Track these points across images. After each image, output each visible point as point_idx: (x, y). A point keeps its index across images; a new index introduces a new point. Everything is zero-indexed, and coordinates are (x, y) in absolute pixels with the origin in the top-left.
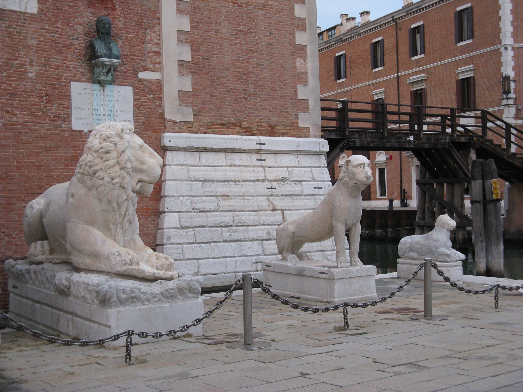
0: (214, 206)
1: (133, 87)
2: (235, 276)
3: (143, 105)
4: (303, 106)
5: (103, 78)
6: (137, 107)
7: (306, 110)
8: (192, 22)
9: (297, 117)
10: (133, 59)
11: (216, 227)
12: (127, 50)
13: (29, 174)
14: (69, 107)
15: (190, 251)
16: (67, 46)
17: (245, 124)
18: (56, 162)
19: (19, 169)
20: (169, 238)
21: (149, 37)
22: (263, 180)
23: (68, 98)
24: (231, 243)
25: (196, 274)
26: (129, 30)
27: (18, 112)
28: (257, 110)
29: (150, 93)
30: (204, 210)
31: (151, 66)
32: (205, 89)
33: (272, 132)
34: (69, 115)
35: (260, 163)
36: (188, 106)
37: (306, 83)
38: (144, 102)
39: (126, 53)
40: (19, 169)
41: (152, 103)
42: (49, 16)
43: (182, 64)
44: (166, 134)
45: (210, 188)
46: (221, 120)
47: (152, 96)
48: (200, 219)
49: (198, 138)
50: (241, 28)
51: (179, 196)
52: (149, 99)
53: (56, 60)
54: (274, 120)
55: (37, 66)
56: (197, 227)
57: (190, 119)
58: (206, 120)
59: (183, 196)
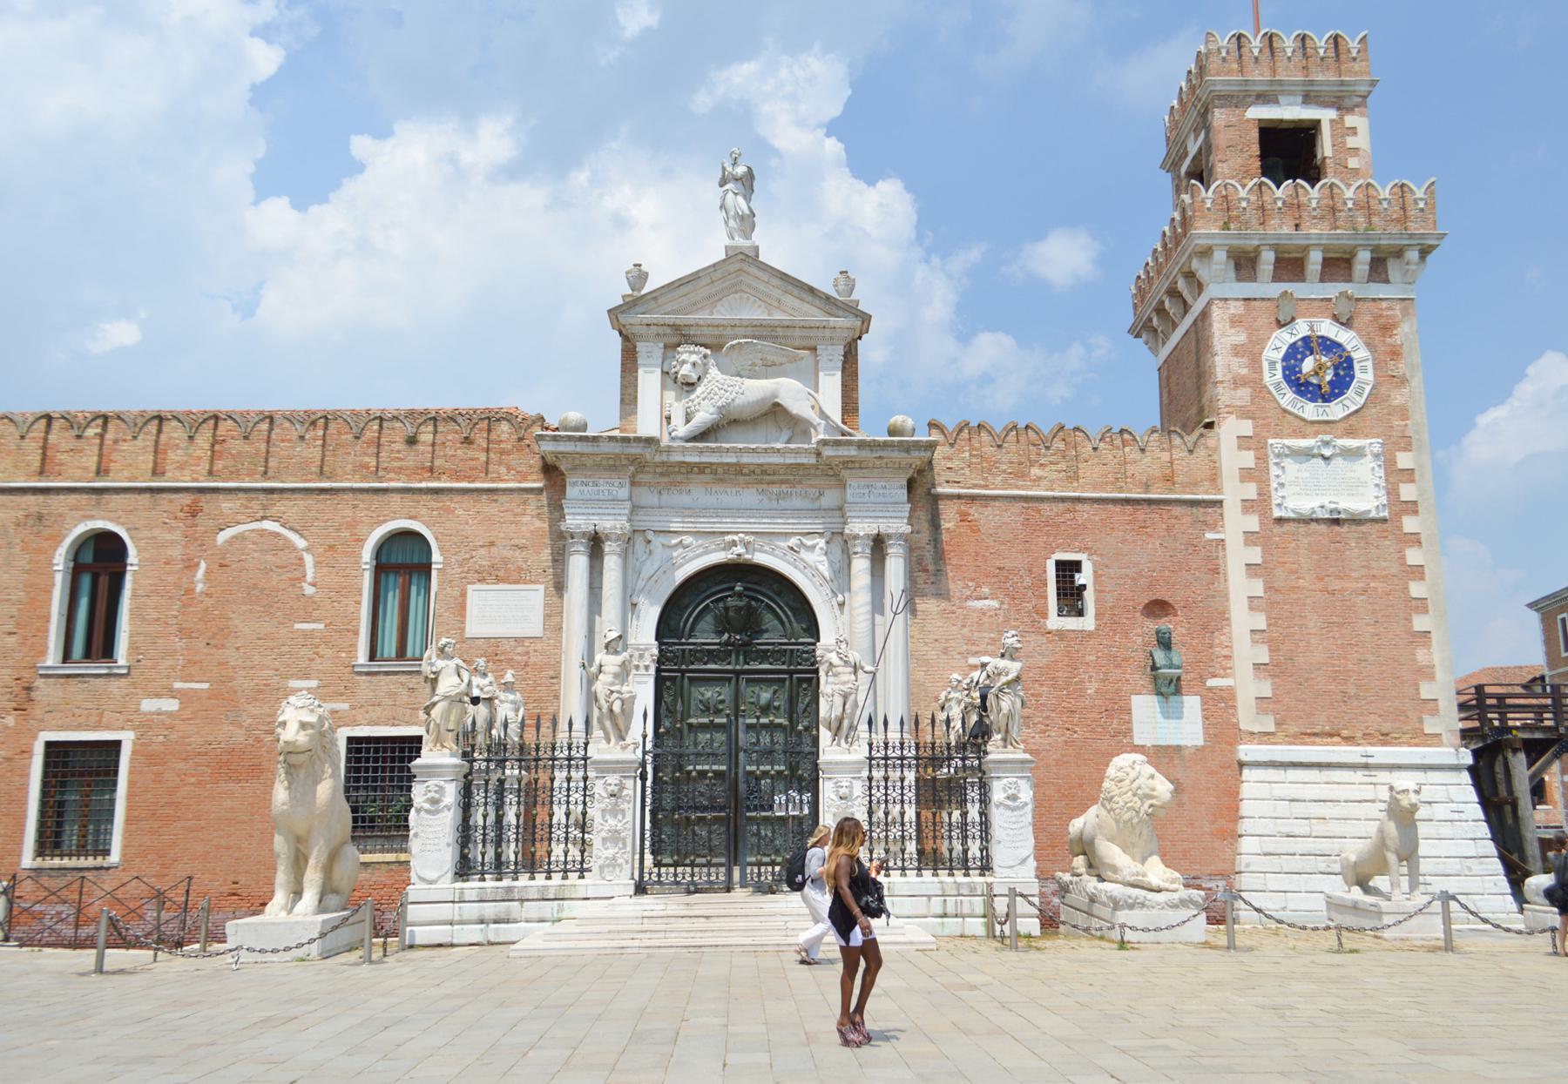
0: (1305, 830)
4: (1431, 706)
5: (1163, 690)
6: (1206, 718)
7: (1435, 712)
8: (1269, 618)
9: (1421, 721)
14: (1130, 722)
15: (1274, 882)
16: (1126, 660)
17: (1345, 733)
19: (1080, 786)
20: (1248, 865)
22: (1373, 801)
23: (1128, 711)
25: (1284, 909)
28: (1362, 715)
33: (1385, 739)
34: (1130, 730)
35: (1369, 780)
37: (1432, 677)
43: (1257, 666)
44: (1241, 747)
45: (1299, 809)
50: (1334, 619)
53: (1115, 674)
54: (1386, 727)
57: (1272, 728)
58: (1293, 729)
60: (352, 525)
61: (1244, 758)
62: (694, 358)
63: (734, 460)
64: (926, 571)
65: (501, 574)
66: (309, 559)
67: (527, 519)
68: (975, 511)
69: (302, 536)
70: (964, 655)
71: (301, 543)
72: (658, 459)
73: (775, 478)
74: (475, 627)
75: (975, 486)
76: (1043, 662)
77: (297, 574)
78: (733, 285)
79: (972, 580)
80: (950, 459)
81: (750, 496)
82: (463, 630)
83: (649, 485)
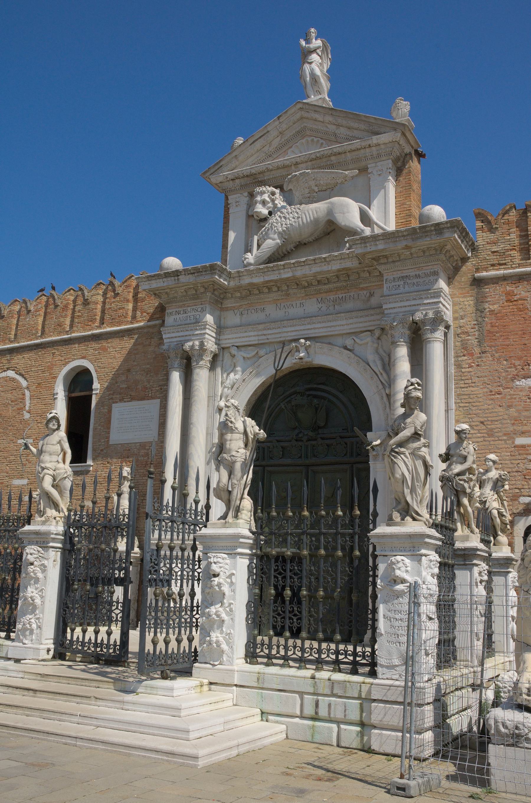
60: (50, 368)
62: (266, 197)
63: (289, 275)
64: (472, 355)
65: (133, 394)
66: (27, 393)
67: (151, 349)
68: (521, 290)
69: (25, 379)
70: (511, 435)
71: (24, 383)
72: (232, 284)
73: (331, 286)
74: (116, 436)
75: (520, 266)
77: (21, 405)
78: (298, 132)
79: (520, 358)
80: (495, 243)
81: (312, 306)
82: (108, 438)
83: (233, 309)
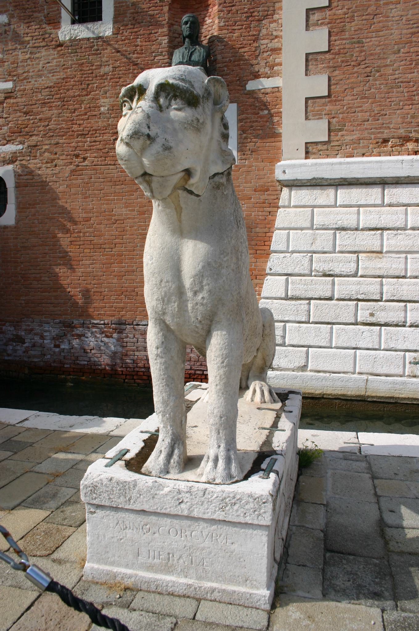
0: (351, 268)
1: (238, 104)
2: (367, 380)
3: (252, 127)
10: (239, 65)
11: (350, 300)
12: (230, 55)
13: (97, 226)
18: (129, 210)
21: (264, 31)
24: (372, 328)
26: (233, 28)
27: (88, 155)
29: (264, 108)
30: (331, 273)
31: (267, 69)
32: (353, 88)
36: (321, 118)
38: (254, 122)
39: (228, 59)
40: (88, 219)
41: (267, 122)
42: (126, 34)
46: (379, 133)
47: (266, 112)
48: (322, 287)
49: (340, 163)
51: (293, 252)
52: (261, 117)
55: (111, 97)
56: (316, 299)
59: (299, 252)
61: (279, 175)
76: (53, 79)
